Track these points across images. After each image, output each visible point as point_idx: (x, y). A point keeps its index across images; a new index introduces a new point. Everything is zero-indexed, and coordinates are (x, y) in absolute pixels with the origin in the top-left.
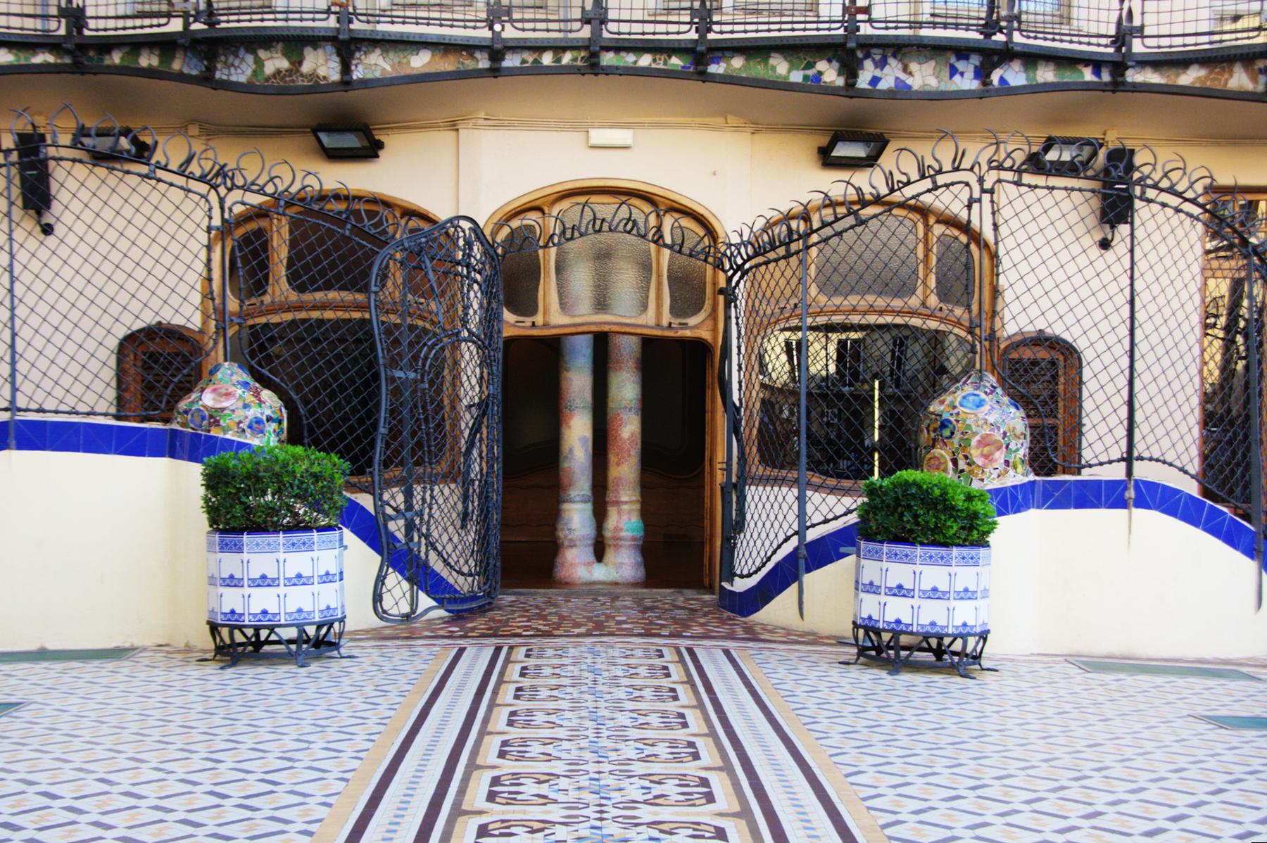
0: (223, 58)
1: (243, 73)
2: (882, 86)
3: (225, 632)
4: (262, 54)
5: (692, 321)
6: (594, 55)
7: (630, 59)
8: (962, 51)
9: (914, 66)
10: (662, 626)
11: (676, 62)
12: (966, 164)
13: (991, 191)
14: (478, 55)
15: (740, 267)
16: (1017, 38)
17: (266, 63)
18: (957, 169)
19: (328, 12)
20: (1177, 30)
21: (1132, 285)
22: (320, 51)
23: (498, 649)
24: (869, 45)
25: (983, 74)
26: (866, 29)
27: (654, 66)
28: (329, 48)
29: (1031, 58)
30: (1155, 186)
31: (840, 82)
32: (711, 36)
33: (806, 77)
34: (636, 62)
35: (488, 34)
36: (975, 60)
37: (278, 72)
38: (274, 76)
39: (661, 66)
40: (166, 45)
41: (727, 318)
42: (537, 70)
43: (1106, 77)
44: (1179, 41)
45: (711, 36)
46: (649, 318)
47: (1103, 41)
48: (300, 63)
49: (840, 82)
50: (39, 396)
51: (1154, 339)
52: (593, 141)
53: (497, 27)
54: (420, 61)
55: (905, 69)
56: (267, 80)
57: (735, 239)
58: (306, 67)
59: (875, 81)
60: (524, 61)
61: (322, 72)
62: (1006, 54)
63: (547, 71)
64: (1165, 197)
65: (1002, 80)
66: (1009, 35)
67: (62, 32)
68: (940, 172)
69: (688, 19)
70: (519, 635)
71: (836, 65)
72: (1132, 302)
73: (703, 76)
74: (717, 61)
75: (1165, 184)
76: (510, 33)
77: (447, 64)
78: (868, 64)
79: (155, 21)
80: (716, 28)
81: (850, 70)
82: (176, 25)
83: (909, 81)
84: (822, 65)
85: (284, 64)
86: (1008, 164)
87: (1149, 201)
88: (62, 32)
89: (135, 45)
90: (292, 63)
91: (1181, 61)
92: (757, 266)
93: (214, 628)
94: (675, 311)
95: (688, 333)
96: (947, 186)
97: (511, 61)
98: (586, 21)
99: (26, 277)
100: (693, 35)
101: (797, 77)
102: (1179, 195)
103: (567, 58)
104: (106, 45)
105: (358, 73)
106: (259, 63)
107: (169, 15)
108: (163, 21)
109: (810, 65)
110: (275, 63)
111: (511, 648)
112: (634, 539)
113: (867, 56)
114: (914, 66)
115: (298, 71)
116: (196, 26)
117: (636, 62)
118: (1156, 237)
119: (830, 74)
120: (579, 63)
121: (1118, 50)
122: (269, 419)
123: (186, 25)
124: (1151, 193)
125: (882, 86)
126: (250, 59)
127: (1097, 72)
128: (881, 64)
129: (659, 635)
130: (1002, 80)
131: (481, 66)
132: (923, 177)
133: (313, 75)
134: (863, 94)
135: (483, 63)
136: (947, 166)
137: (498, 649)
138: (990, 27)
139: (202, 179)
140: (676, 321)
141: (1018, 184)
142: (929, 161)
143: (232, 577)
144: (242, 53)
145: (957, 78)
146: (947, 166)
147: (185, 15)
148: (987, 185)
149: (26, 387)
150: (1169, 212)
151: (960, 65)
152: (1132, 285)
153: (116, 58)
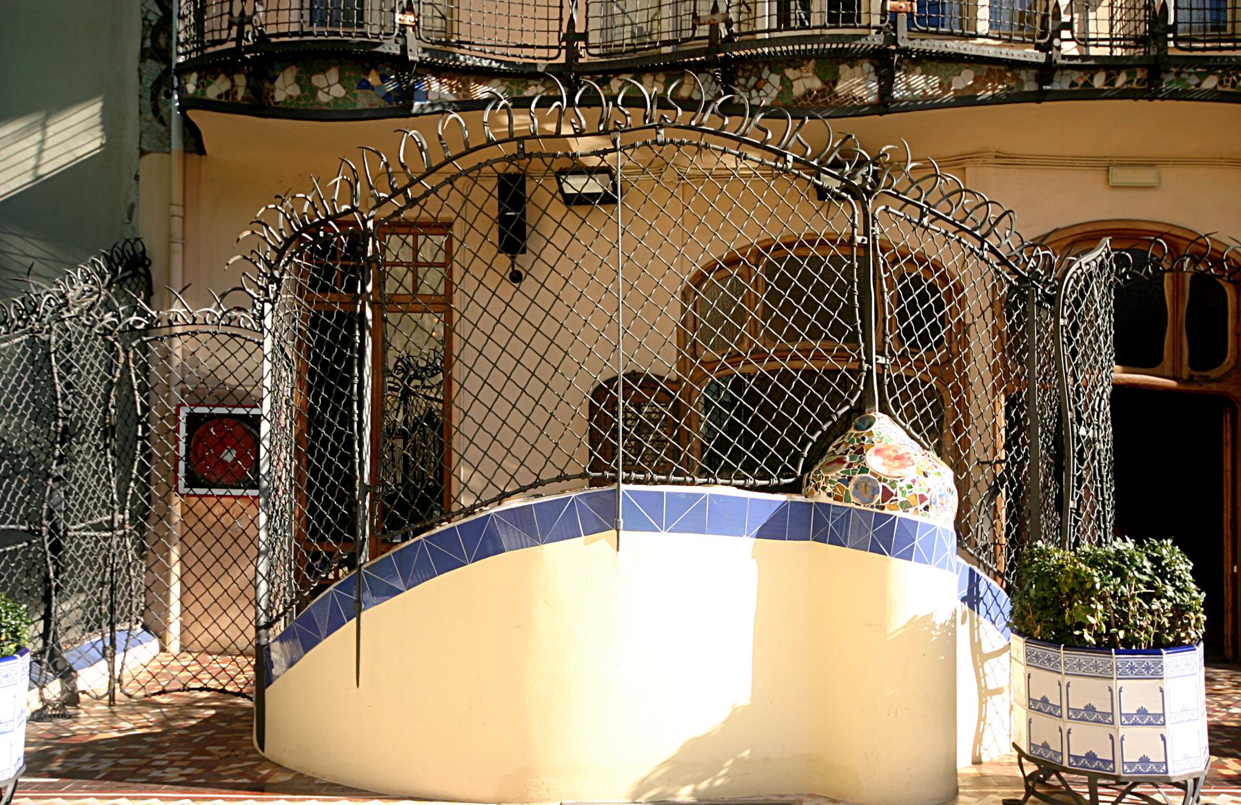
0: (742, 81)
1: (767, 95)
4: (790, 73)
14: (1023, 75)
17: (795, 83)
22: (857, 69)
27: (1220, 88)
28: (867, 66)
34: (1198, 85)
37: (810, 92)
38: (804, 97)
39: (1229, 89)
42: (1088, 93)
48: (835, 83)
54: (964, 80)
56: (795, 102)
58: (840, 88)
60: (1073, 84)
61: (858, 92)
63: (1096, 95)
85: (817, 84)
90: (824, 83)
94: (1193, 364)
97: (1061, 83)
103: (1121, 81)
106: (787, 84)
110: (806, 82)
115: (831, 91)
117: (1198, 85)
120: (1134, 86)
126: (775, 79)
131: (1026, 89)
140: (1196, 374)
144: (765, 73)
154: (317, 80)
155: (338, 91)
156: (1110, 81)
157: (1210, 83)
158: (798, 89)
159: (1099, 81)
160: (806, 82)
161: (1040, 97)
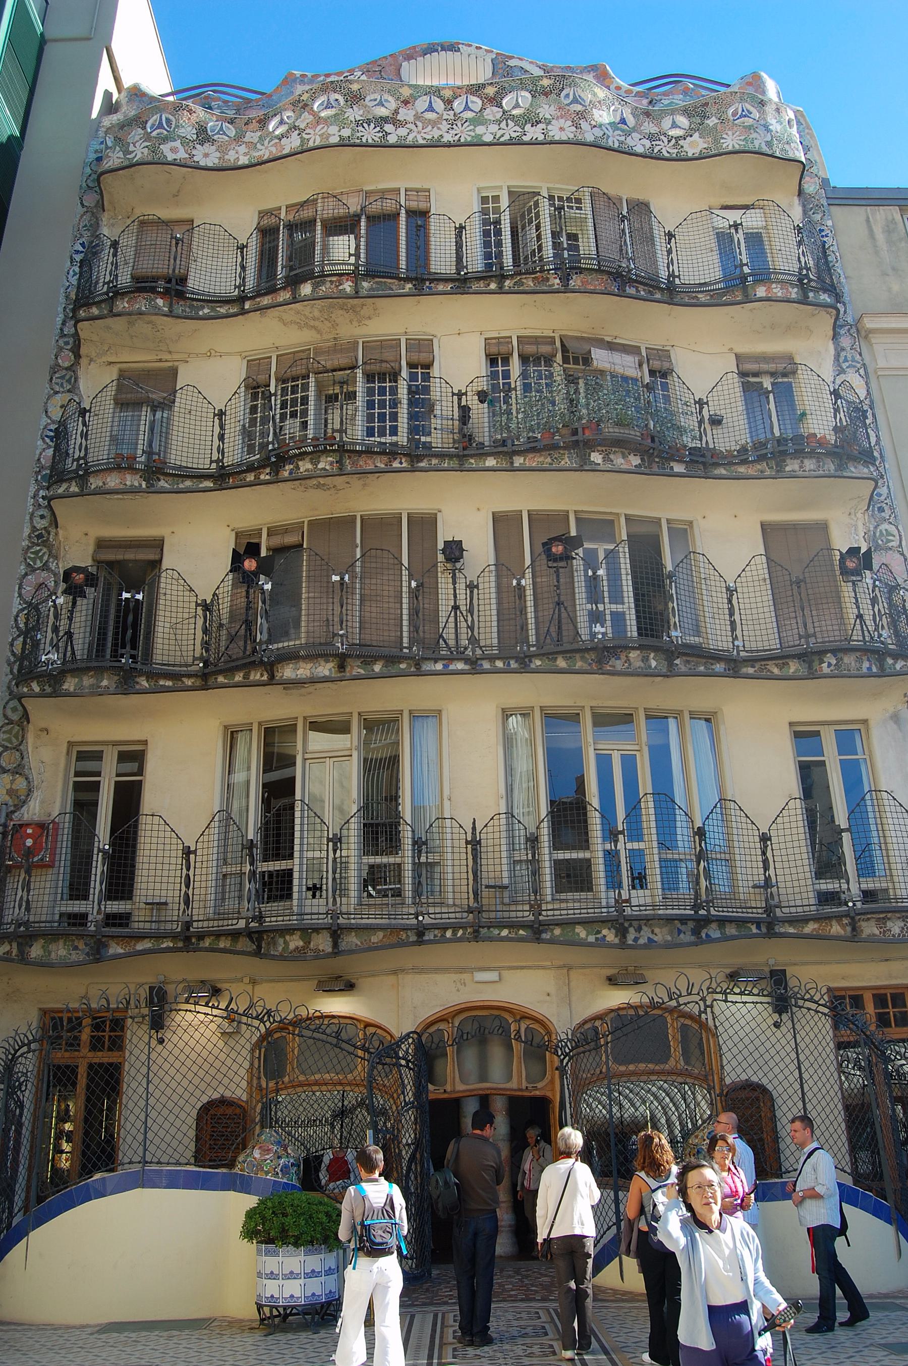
2: (641, 941)
3: (267, 1310)
4: (288, 937)
5: (540, 1085)
6: (476, 931)
7: (496, 932)
8: (683, 920)
9: (657, 930)
10: (536, 1292)
11: (521, 932)
12: (695, 991)
13: (711, 1006)
14: (409, 933)
15: (567, 1054)
16: (713, 912)
18: (690, 994)
19: (327, 913)
20: (799, 903)
21: (798, 1057)
23: (436, 1316)
24: (630, 919)
25: (696, 932)
26: (628, 911)
29: (722, 922)
30: (803, 999)
31: (617, 941)
32: (541, 918)
33: (597, 939)
35: (415, 921)
36: (691, 924)
40: (235, 935)
41: (562, 1085)
42: (443, 940)
43: (764, 930)
44: (800, 909)
45: (541, 918)
46: (514, 1084)
47: (760, 911)
49: (617, 941)
50: (159, 1154)
51: (815, 1089)
52: (476, 979)
53: (420, 918)
55: (653, 932)
57: (563, 1036)
59: (636, 939)
60: (435, 936)
62: (706, 921)
63: (450, 941)
64: (808, 1004)
65: (707, 935)
66: (708, 911)
67: (179, 930)
68: (680, 996)
69: (527, 907)
70: (446, 1303)
71: (613, 931)
72: (799, 1068)
73: (538, 940)
74: (545, 931)
75: (807, 996)
76: (427, 920)
77: (394, 939)
78: (631, 930)
79: (230, 922)
80: (544, 913)
81: (622, 932)
82: (242, 924)
83: (656, 939)
84: (605, 932)
85: (301, 943)
86: (719, 990)
87: (800, 1007)
88: (179, 930)
89: (218, 935)
91: (805, 920)
92: (579, 1054)
93: (260, 1307)
95: (538, 1093)
96: (685, 1004)
97: (429, 936)
98: (470, 911)
99: (156, 1081)
100: (532, 918)
101: (591, 939)
102: (816, 1002)
103: (460, 933)
104: (201, 937)
105: (343, 946)
107: (238, 919)
108: (235, 922)
109: (599, 932)
110: (295, 942)
111: (443, 1314)
112: (510, 1226)
113: (631, 925)
114: (657, 930)
116: (252, 924)
118: (807, 1028)
119: (610, 935)
121: (768, 915)
122: (293, 1165)
123: (247, 923)
124: (800, 1003)
125: (641, 941)
126: (281, 941)
127: (758, 927)
128: (639, 929)
129: (534, 1300)
130: (707, 935)
132: (671, 999)
133: (317, 950)
134: (630, 947)
135: (413, 938)
136: (684, 993)
137: (436, 1316)
138: (696, 907)
139: (257, 1018)
140: (530, 1086)
141: (726, 1001)
142: (673, 990)
143: (272, 1273)
145: (682, 935)
146: (684, 993)
147: (247, 918)
148: (708, 1003)
149: (152, 1148)
150: (812, 1013)
151: (683, 928)
152: (798, 1057)
153: (207, 943)
154: (52, 947)
155: (62, 952)
156: (454, 933)
157: (505, 932)
158: (292, 946)
159: (449, 934)
160: (295, 942)
161: (420, 942)
